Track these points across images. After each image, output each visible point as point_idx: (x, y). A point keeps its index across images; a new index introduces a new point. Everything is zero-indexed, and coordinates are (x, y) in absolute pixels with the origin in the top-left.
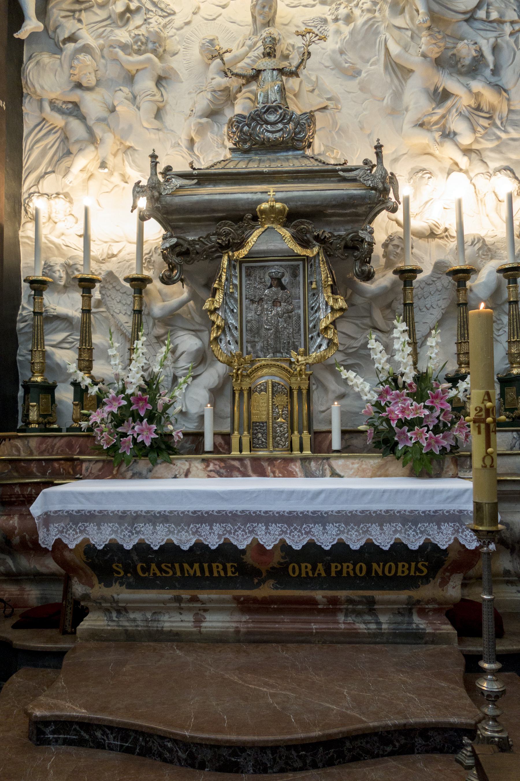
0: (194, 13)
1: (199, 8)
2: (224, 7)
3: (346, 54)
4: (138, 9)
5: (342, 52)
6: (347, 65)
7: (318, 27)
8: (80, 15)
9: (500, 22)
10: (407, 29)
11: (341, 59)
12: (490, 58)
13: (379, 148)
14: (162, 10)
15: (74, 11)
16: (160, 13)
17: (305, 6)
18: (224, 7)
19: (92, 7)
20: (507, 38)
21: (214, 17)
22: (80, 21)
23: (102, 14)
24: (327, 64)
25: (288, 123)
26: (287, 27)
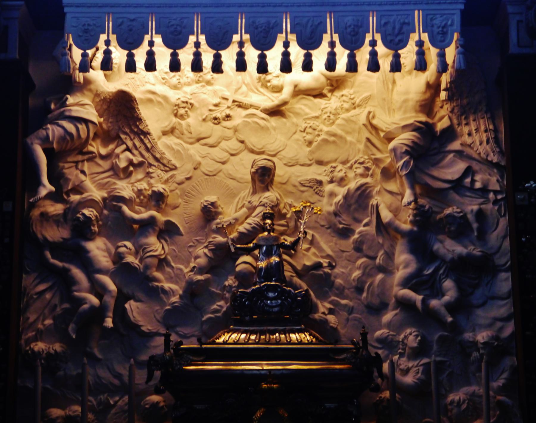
0: (195, 169)
1: (200, 164)
2: (223, 163)
3: (340, 217)
4: (140, 164)
5: (336, 214)
6: (341, 226)
7: (315, 188)
8: (83, 165)
9: (484, 191)
10: (397, 194)
11: (335, 220)
12: (475, 226)
13: (364, 336)
14: (164, 165)
15: (77, 163)
16: (162, 168)
17: (302, 165)
18: (223, 163)
19: (95, 157)
20: (490, 206)
21: (214, 173)
22: (83, 172)
23: (106, 165)
24: (323, 223)
25: (286, 299)
26: (284, 186)
